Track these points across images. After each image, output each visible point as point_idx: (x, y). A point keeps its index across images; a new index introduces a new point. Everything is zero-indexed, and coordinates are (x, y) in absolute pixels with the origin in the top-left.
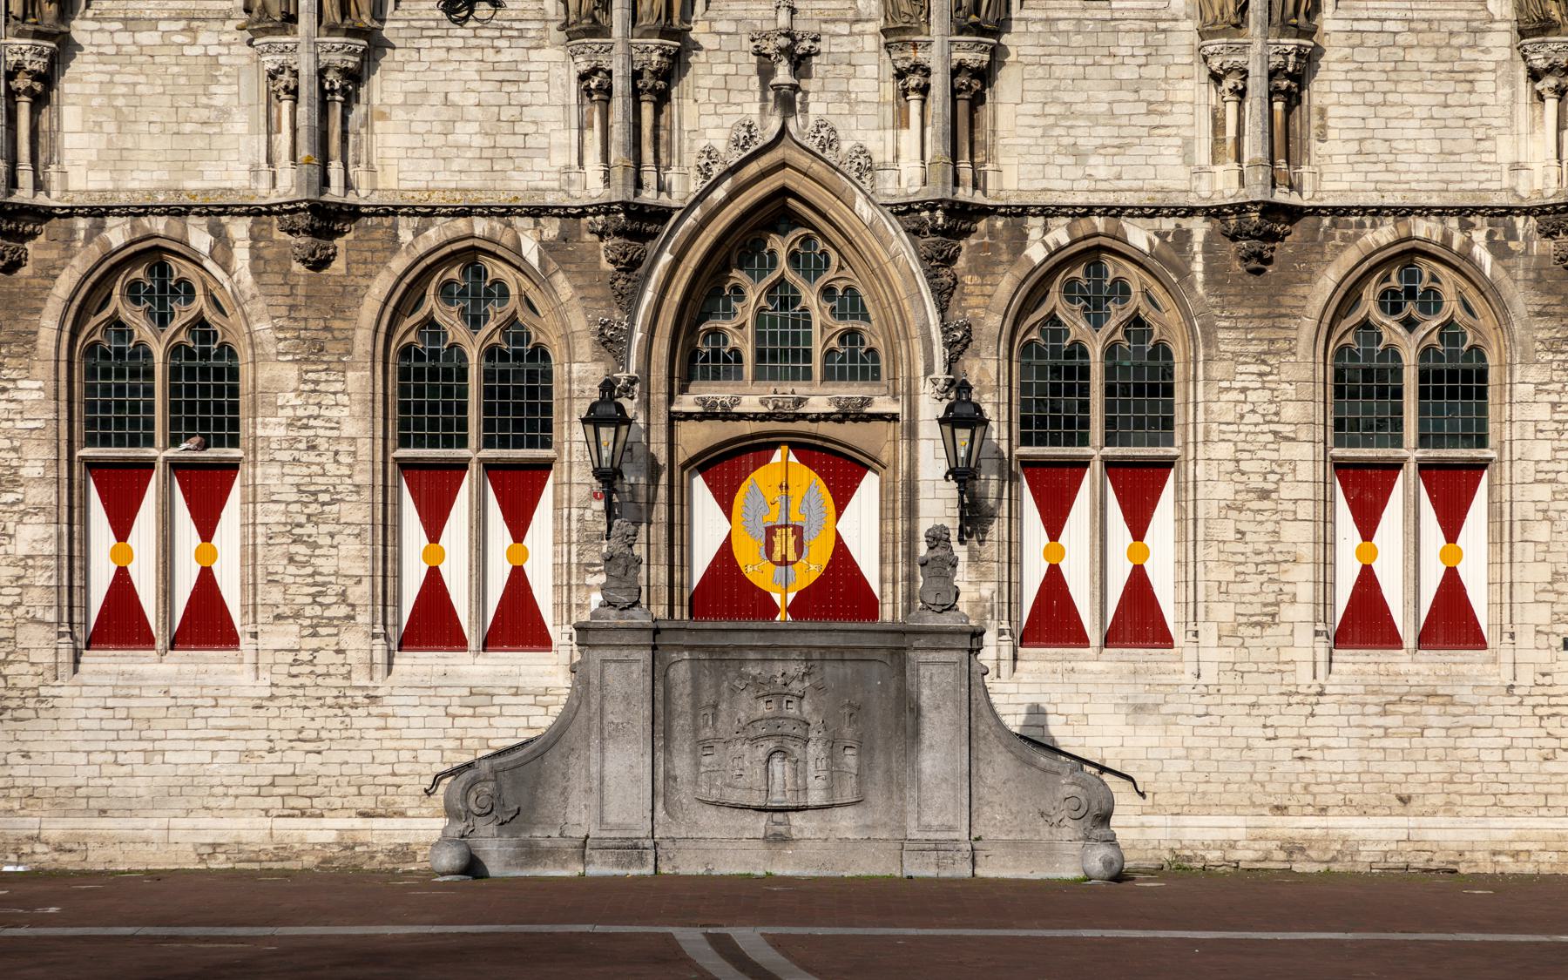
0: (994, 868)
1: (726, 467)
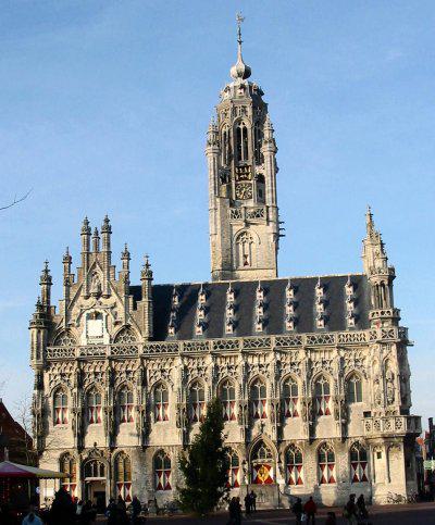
1: (258, 467)
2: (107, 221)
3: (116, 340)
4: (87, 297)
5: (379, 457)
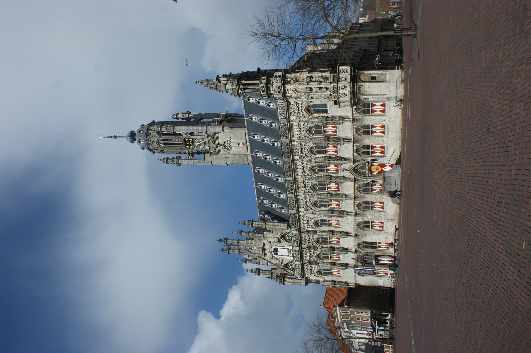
0: (400, 171)
1: (371, 172)
2: (220, 240)
3: (289, 241)
4: (265, 255)
5: (368, 98)
